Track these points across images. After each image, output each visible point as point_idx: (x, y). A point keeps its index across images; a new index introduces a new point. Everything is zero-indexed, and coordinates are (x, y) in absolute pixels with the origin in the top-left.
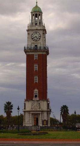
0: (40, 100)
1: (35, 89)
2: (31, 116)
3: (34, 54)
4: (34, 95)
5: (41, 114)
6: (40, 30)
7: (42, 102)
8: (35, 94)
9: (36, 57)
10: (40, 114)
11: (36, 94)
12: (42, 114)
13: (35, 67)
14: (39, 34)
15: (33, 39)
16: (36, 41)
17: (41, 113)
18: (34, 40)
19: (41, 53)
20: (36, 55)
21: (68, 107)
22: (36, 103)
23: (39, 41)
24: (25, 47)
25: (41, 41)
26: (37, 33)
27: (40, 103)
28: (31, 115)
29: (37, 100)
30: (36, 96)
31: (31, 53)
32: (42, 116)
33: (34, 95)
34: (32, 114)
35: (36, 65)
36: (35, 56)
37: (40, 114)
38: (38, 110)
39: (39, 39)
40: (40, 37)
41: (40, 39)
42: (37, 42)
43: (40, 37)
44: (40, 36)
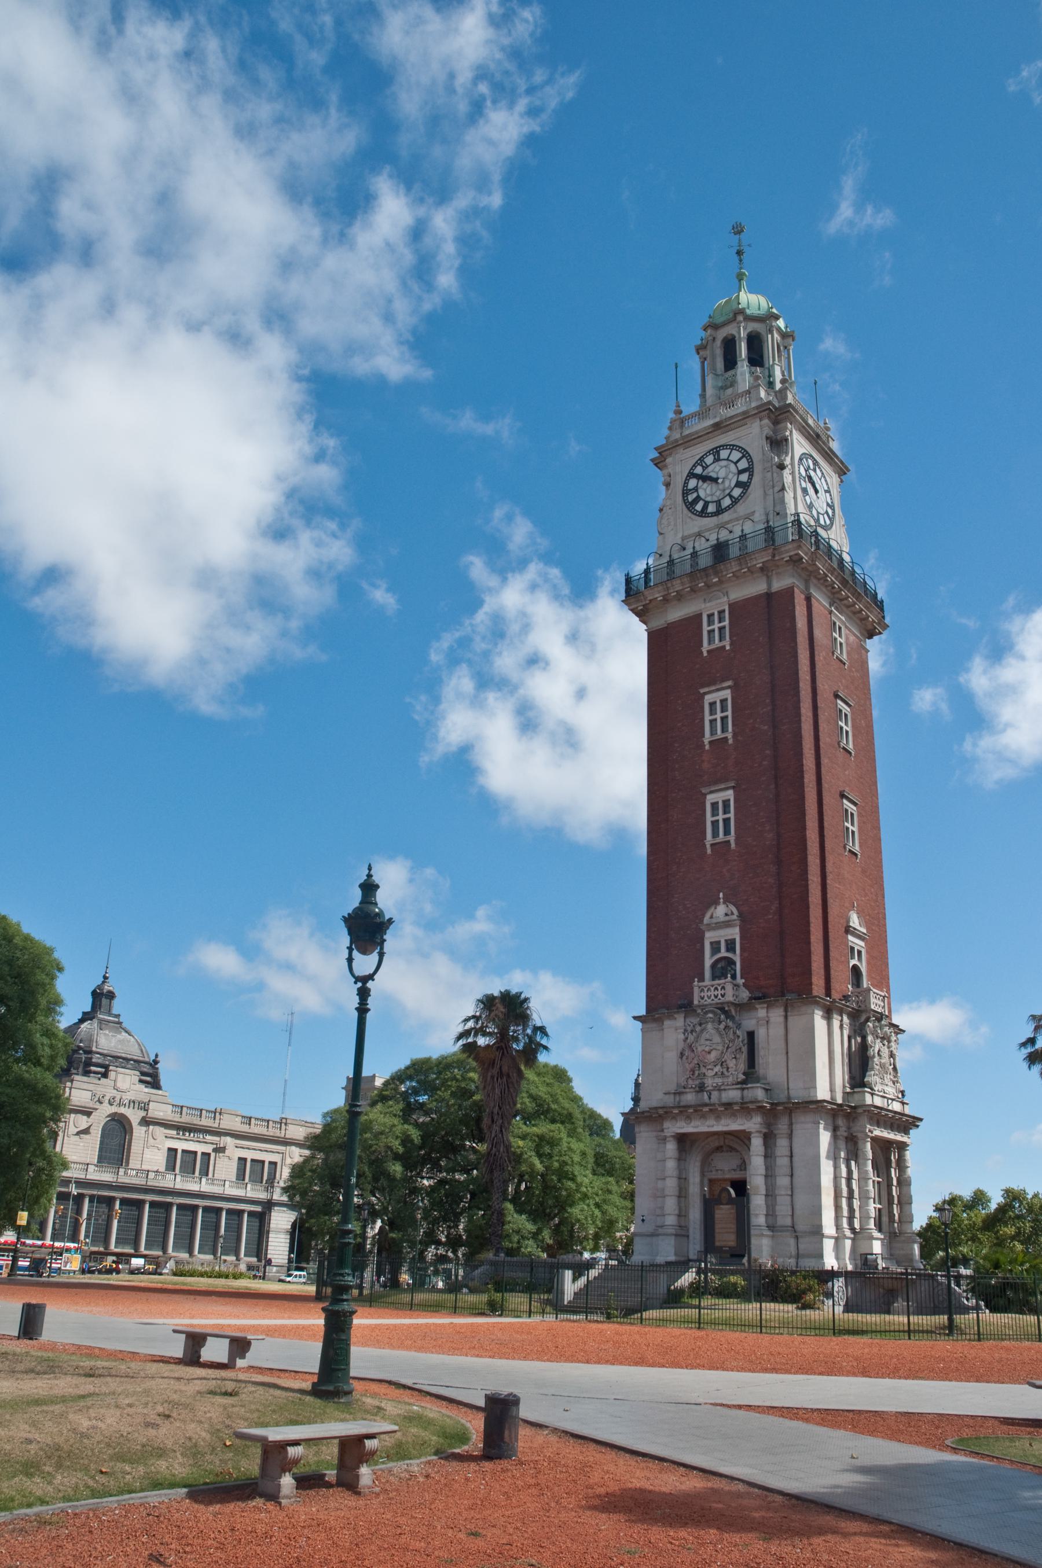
0: (760, 996)
1: (716, 903)
2: (671, 1165)
3: (699, 616)
4: (708, 962)
5: (757, 1143)
6: (746, 417)
7: (777, 1015)
8: (715, 947)
9: (714, 638)
10: (744, 1138)
11: (723, 953)
12: (769, 1138)
13: (712, 712)
14: (736, 455)
15: (699, 507)
16: (720, 511)
17: (753, 1124)
18: (703, 514)
19: (756, 588)
20: (712, 610)
21: (377, 887)
22: (712, 1039)
23: (741, 509)
24: (628, 581)
25: (755, 502)
26: (724, 454)
27: (761, 1034)
28: (671, 1147)
29: (722, 1009)
30: (722, 969)
31: (676, 614)
32: (769, 1155)
33: (708, 962)
34: (682, 1139)
35: (716, 697)
36: (710, 623)
37: (744, 1138)
38: (733, 1095)
39: (737, 492)
40: (744, 478)
41: (744, 486)
42: (725, 517)
43: (744, 478)
44: (743, 464)
